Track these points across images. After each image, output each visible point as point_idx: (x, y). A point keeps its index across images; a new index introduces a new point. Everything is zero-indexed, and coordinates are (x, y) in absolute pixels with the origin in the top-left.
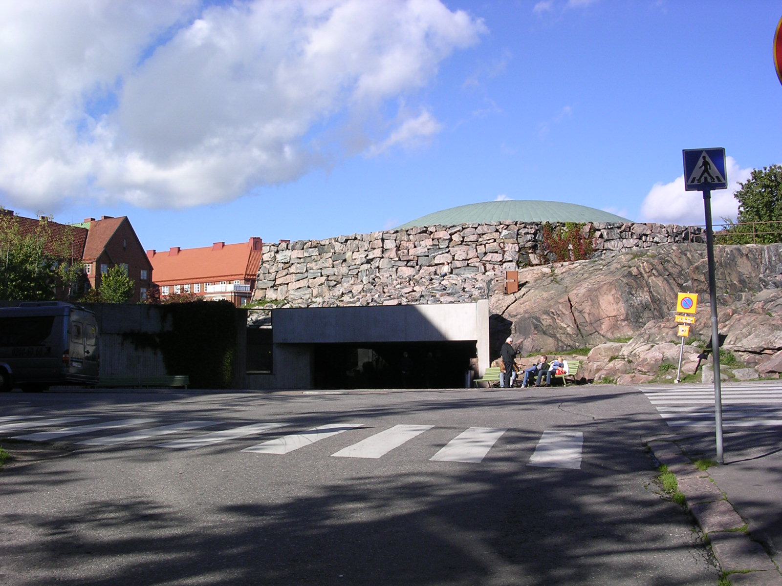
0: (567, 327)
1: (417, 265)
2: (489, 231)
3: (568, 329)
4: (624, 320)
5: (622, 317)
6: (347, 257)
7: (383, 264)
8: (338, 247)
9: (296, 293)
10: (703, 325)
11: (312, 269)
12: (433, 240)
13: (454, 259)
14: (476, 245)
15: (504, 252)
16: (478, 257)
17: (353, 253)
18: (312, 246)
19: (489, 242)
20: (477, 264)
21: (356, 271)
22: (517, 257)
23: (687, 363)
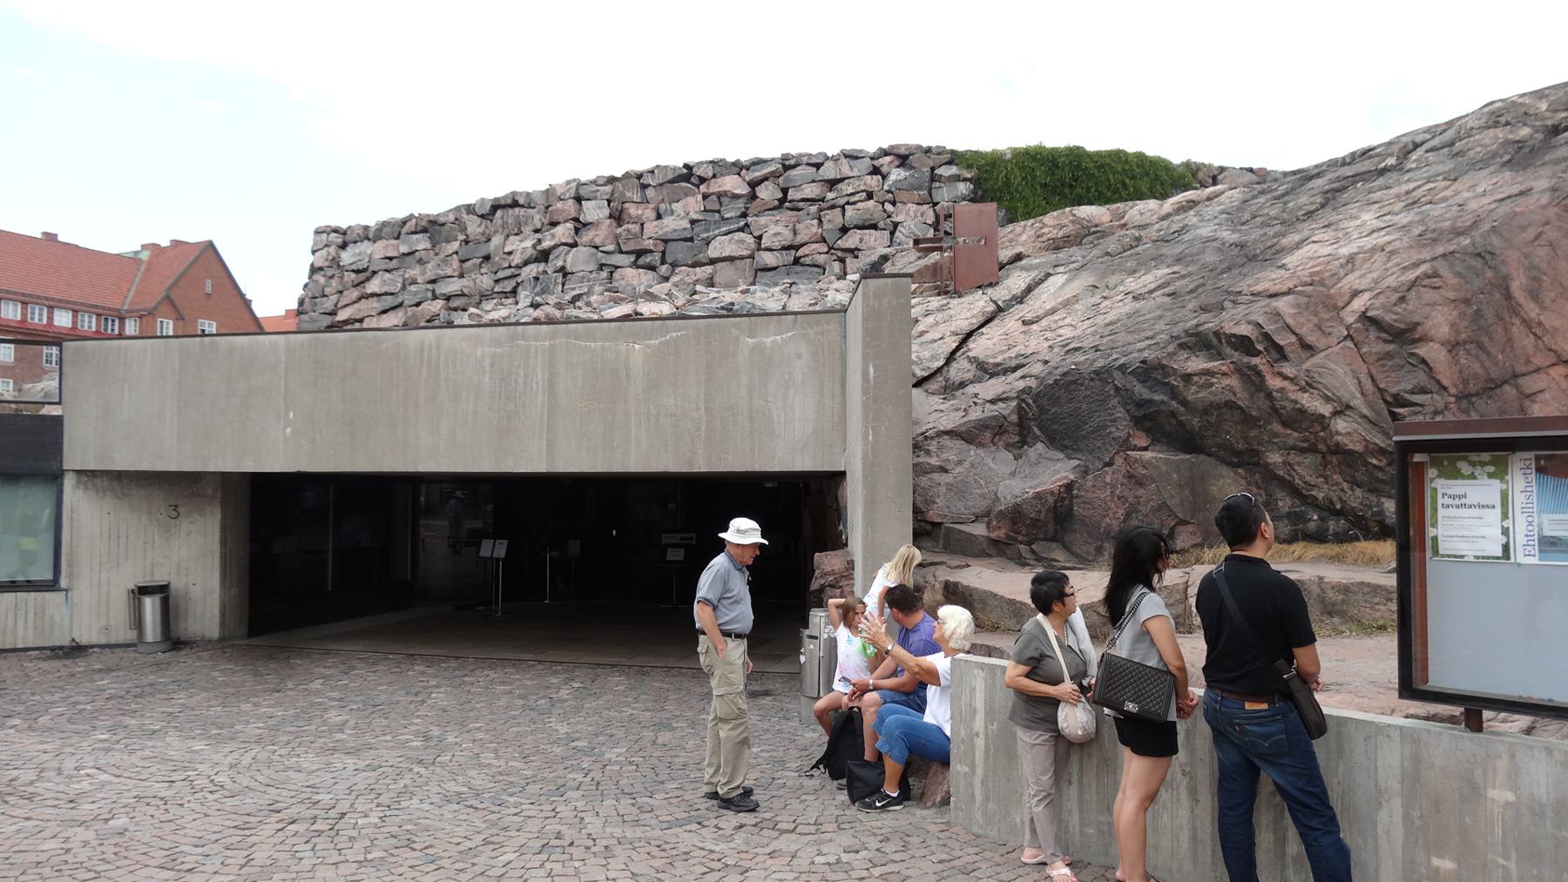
0: (1336, 413)
1: (663, 262)
2: (855, 174)
3: (1341, 425)
7: (578, 259)
8: (474, 227)
12: (705, 197)
15: (896, 225)
16: (824, 240)
20: (821, 259)
21: (512, 283)
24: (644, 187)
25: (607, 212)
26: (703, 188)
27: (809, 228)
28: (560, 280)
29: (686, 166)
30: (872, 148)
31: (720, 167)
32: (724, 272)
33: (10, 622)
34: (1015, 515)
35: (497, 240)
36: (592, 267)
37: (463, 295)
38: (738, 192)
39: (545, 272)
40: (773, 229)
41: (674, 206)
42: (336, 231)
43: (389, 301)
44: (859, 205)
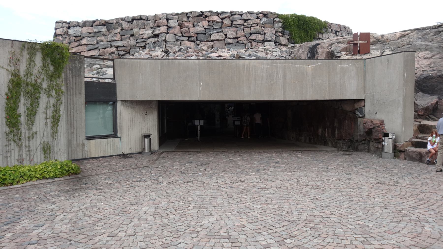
1: (197, 40)
6: (135, 32)
7: (170, 37)
8: (125, 25)
11: (102, 41)
12: (209, 22)
13: (226, 37)
14: (244, 28)
15: (265, 33)
16: (245, 36)
17: (140, 29)
18: (101, 24)
19: (253, 25)
20: (245, 42)
21: (144, 44)
22: (274, 38)
24: (188, 17)
25: (177, 24)
26: (207, 19)
27: (241, 33)
28: (165, 44)
29: (201, 12)
31: (212, 13)
32: (216, 44)
33: (106, 148)
34: (426, 109)
36: (174, 40)
38: (218, 21)
40: (230, 33)
41: (199, 23)
42: (65, 22)
43: (91, 47)
44: (255, 27)
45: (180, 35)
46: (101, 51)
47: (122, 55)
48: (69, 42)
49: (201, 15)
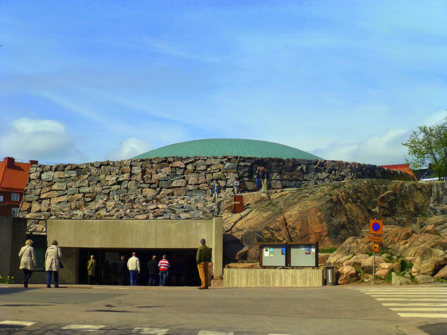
1: (158, 187)
4: (326, 236)
5: (325, 234)
6: (101, 178)
8: (94, 170)
9: (57, 206)
10: (390, 241)
12: (171, 167)
14: (206, 174)
15: (227, 179)
16: (206, 182)
17: (106, 176)
20: (206, 188)
21: (108, 191)
23: (379, 269)
24: (152, 163)
25: (141, 171)
29: (165, 158)
30: (221, 156)
35: (102, 176)
36: (136, 187)
37: (90, 193)
38: (181, 167)
39: (120, 188)
40: (192, 179)
45: (142, 182)
46: (70, 197)
47: (88, 202)
48: (41, 186)
49: (165, 161)
